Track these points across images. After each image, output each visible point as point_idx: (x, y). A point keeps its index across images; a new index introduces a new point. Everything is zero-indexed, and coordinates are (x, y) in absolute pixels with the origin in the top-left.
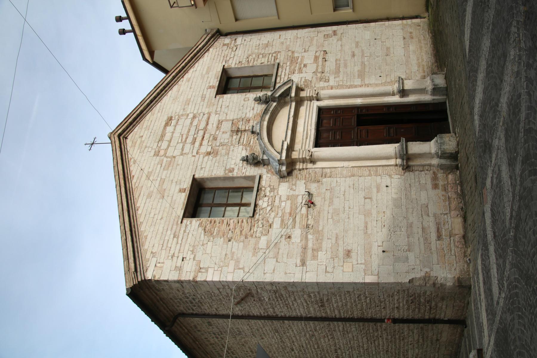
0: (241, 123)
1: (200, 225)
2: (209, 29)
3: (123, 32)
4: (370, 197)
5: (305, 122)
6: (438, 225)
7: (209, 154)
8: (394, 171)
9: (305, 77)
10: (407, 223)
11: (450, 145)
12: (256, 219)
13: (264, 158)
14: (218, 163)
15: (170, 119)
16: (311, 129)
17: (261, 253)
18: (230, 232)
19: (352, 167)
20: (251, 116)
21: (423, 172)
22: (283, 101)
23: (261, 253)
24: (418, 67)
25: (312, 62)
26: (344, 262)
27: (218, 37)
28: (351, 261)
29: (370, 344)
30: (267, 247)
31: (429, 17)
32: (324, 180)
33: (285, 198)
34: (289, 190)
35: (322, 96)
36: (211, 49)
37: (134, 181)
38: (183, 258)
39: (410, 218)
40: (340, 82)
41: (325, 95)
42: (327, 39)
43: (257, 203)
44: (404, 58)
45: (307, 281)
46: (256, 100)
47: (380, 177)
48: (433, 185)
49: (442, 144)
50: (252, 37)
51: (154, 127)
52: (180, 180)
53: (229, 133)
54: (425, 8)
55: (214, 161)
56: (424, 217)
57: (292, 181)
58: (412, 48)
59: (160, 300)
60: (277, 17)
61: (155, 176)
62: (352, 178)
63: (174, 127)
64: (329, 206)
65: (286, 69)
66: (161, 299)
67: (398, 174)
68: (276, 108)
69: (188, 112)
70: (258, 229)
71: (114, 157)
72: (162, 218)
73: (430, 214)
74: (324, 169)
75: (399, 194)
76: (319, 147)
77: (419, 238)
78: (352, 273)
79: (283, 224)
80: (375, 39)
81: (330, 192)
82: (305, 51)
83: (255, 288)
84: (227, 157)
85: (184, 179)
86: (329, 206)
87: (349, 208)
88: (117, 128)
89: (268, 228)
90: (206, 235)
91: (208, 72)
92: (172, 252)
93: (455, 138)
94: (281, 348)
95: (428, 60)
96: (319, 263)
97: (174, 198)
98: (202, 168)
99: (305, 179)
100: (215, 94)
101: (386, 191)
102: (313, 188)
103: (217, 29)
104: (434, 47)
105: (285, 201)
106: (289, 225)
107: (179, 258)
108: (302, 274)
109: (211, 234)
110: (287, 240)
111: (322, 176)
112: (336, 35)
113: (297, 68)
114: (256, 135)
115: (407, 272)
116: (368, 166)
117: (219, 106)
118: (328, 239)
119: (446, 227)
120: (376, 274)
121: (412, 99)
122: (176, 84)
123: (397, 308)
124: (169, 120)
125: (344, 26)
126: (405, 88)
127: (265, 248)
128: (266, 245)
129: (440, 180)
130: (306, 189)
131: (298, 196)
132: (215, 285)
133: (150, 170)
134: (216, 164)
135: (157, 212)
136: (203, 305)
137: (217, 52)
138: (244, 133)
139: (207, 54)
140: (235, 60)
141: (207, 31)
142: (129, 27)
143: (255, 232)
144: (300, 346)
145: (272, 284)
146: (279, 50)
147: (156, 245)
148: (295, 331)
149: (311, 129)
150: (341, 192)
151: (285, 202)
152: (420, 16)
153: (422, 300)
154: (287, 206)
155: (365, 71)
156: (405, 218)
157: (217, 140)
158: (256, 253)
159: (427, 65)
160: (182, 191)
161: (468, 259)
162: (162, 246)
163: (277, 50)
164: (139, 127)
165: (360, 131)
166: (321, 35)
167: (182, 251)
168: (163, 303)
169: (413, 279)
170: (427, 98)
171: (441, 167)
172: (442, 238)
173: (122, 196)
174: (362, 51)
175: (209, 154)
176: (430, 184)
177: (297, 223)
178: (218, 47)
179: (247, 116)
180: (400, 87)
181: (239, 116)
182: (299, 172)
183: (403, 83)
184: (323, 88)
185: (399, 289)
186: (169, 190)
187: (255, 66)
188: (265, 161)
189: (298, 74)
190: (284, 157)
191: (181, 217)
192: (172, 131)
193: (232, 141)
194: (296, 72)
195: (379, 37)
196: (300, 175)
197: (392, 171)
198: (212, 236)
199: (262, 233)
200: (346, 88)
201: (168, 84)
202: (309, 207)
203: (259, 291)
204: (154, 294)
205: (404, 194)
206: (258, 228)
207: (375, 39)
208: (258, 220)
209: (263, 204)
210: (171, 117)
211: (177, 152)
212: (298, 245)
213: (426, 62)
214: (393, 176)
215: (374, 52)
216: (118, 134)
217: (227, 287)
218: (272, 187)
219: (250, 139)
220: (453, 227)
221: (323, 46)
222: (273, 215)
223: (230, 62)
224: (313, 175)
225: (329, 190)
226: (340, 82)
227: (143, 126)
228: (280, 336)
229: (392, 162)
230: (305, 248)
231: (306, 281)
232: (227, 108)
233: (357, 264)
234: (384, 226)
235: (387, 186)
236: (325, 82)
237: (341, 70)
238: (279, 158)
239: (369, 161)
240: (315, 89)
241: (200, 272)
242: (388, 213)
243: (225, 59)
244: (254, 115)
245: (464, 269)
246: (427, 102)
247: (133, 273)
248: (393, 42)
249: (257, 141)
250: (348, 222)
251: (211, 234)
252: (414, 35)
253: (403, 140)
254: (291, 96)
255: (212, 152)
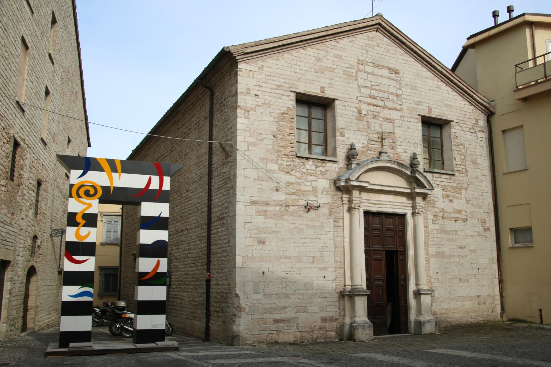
0: (390, 141)
1: (288, 108)
2: (495, 104)
3: (495, 15)
4: (315, 262)
5: (389, 202)
6: (288, 321)
7: (359, 112)
8: (339, 283)
9: (438, 201)
10: (290, 294)
11: (362, 334)
12: (294, 159)
13: (353, 165)
14: (350, 122)
15: (397, 73)
16: (382, 207)
17: (262, 165)
18: (282, 136)
19: (344, 246)
20: (398, 150)
21: (337, 309)
22: (412, 181)
23: (262, 165)
24: (446, 308)
25: (454, 208)
26: (254, 238)
27: (486, 113)
28: (255, 244)
29: (191, 260)
30: (268, 170)
31: (503, 321)
32: (332, 221)
33: (314, 185)
34: (323, 188)
35: (416, 218)
36: (472, 107)
37: (333, 43)
38: (258, 95)
39: (294, 296)
40: (433, 234)
41: (418, 220)
42: (480, 222)
43: (309, 160)
44: (457, 296)
45: (237, 206)
46: (414, 154)
47: (334, 270)
48: (326, 317)
49: (363, 327)
50: (484, 147)
51: (389, 57)
52: (332, 87)
53: (380, 130)
54: (512, 318)
55: (351, 117)
56: (295, 308)
57: (331, 191)
58: (468, 304)
59: (223, 74)
60: (505, 172)
61: (337, 63)
62: (333, 246)
63: (388, 76)
64: (306, 225)
65: (448, 182)
66: (224, 75)
67: (336, 287)
68: (405, 175)
69: (403, 89)
70: (285, 161)
71: (357, 22)
72: (296, 73)
73: (297, 314)
74: (342, 220)
75: (317, 287)
76: (364, 215)
77: (276, 303)
78: (244, 245)
79: (289, 184)
80: (478, 269)
81: (319, 226)
82: (467, 200)
83: (232, 161)
84: (356, 129)
85: (334, 90)
86: (306, 225)
87: (304, 243)
88: (387, 21)
89: (286, 170)
90: (279, 115)
91: (447, 106)
92: (263, 85)
93: (369, 339)
94: (188, 181)
95: (453, 318)
96: (253, 217)
97: (315, 83)
98: (345, 106)
99: (332, 203)
100: (423, 114)
101: (319, 276)
102: (324, 210)
103: (494, 112)
104: (468, 325)
105: (311, 185)
106: (288, 189)
107: (258, 91)
108: (244, 202)
109: (280, 120)
110: (275, 187)
111: (335, 218)
112: (484, 231)
113: (448, 193)
114: (378, 156)
115: (245, 293)
116: (344, 260)
117: (409, 119)
118: (275, 224)
119: (286, 328)
120: (243, 266)
121: (412, 301)
122: (434, 75)
123: (218, 283)
124: (395, 71)
125: (494, 238)
126: (422, 296)
127: (267, 169)
128: (269, 169)
129: (330, 324)
130: (323, 203)
131: (317, 197)
132: (234, 125)
133: (343, 57)
134: (349, 120)
135: (301, 68)
136: (219, 113)
137: (469, 114)
138: (380, 144)
139: (467, 103)
140: (460, 131)
141: (493, 102)
142: (500, 20)
143: (282, 159)
144: (190, 198)
145: (235, 176)
146: (469, 175)
147: (270, 70)
148: (201, 194)
149: (382, 207)
150: (320, 235)
151: (310, 185)
152: (504, 312)
153: (223, 305)
154: (307, 188)
155: (443, 258)
156: (295, 292)
157: (373, 119)
158: (263, 161)
159: (448, 317)
160: (322, 89)
161: (256, 344)
162: (269, 75)
163: (469, 173)
164: (389, 42)
165: (381, 253)
166: (484, 216)
167: (265, 93)
168: (221, 78)
169: (239, 297)
170: (413, 316)
171: (342, 326)
172: (275, 324)
173: (317, 34)
174: (466, 256)
175: (359, 112)
176: (326, 315)
177: (290, 196)
178: (475, 114)
179: (398, 146)
180: (423, 291)
181: (397, 139)
182: (340, 197)
183: (427, 294)
184: (426, 218)
185: (231, 285)
186: (323, 78)
187: (452, 152)
188: (351, 166)
189: (442, 194)
190: (352, 183)
191: (297, 90)
192: (384, 76)
193: (372, 133)
194: (444, 193)
195: (480, 272)
196: (337, 198)
197: (339, 281)
198: (279, 120)
199: (282, 165)
200: (425, 240)
201: (434, 67)
202: (305, 207)
203: (230, 164)
204: (227, 70)
205: (317, 292)
206: (286, 161)
207: (478, 269)
208: (294, 161)
209: (309, 165)
210: (398, 73)
211: (361, 82)
212: (270, 198)
213: (452, 316)
214: (334, 282)
215: (464, 268)
216: (381, 22)
217: (233, 136)
218: (325, 173)
219: (374, 150)
220: (285, 333)
221: (472, 218)
222: (299, 174)
223: (458, 127)
224: (337, 210)
225: (322, 225)
226: (433, 234)
227: (389, 46)
228: (197, 180)
229: (348, 282)
230: (267, 204)
231: (237, 206)
232: (407, 127)
233: (252, 250)
234: (287, 274)
235: (325, 277)
236: (433, 220)
237: (445, 236)
238: (352, 179)
239: (350, 261)
240: (424, 211)
241: (245, 111)
242: (299, 277)
243: (461, 122)
244: (398, 153)
245: (247, 341)
246: (408, 315)
247: (243, 51)
248: (475, 286)
249: (371, 157)
250: (291, 242)
251: (280, 120)
252: (482, 306)
253: (368, 292)
254: (416, 188)
255: (361, 115)
